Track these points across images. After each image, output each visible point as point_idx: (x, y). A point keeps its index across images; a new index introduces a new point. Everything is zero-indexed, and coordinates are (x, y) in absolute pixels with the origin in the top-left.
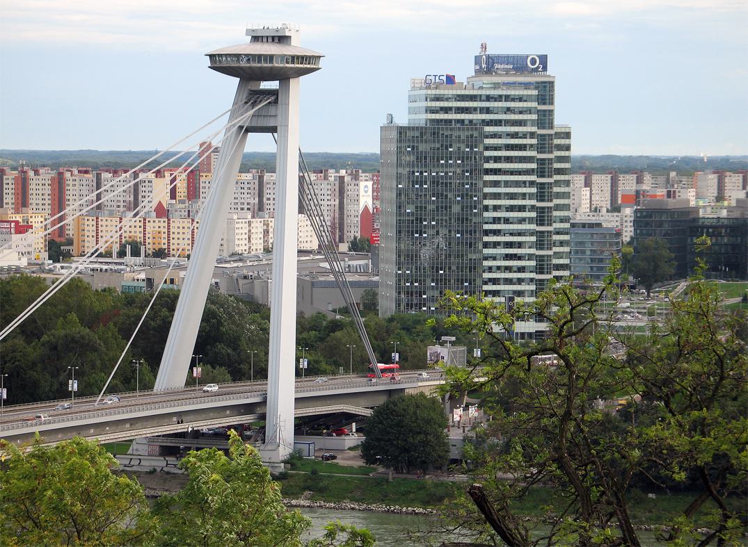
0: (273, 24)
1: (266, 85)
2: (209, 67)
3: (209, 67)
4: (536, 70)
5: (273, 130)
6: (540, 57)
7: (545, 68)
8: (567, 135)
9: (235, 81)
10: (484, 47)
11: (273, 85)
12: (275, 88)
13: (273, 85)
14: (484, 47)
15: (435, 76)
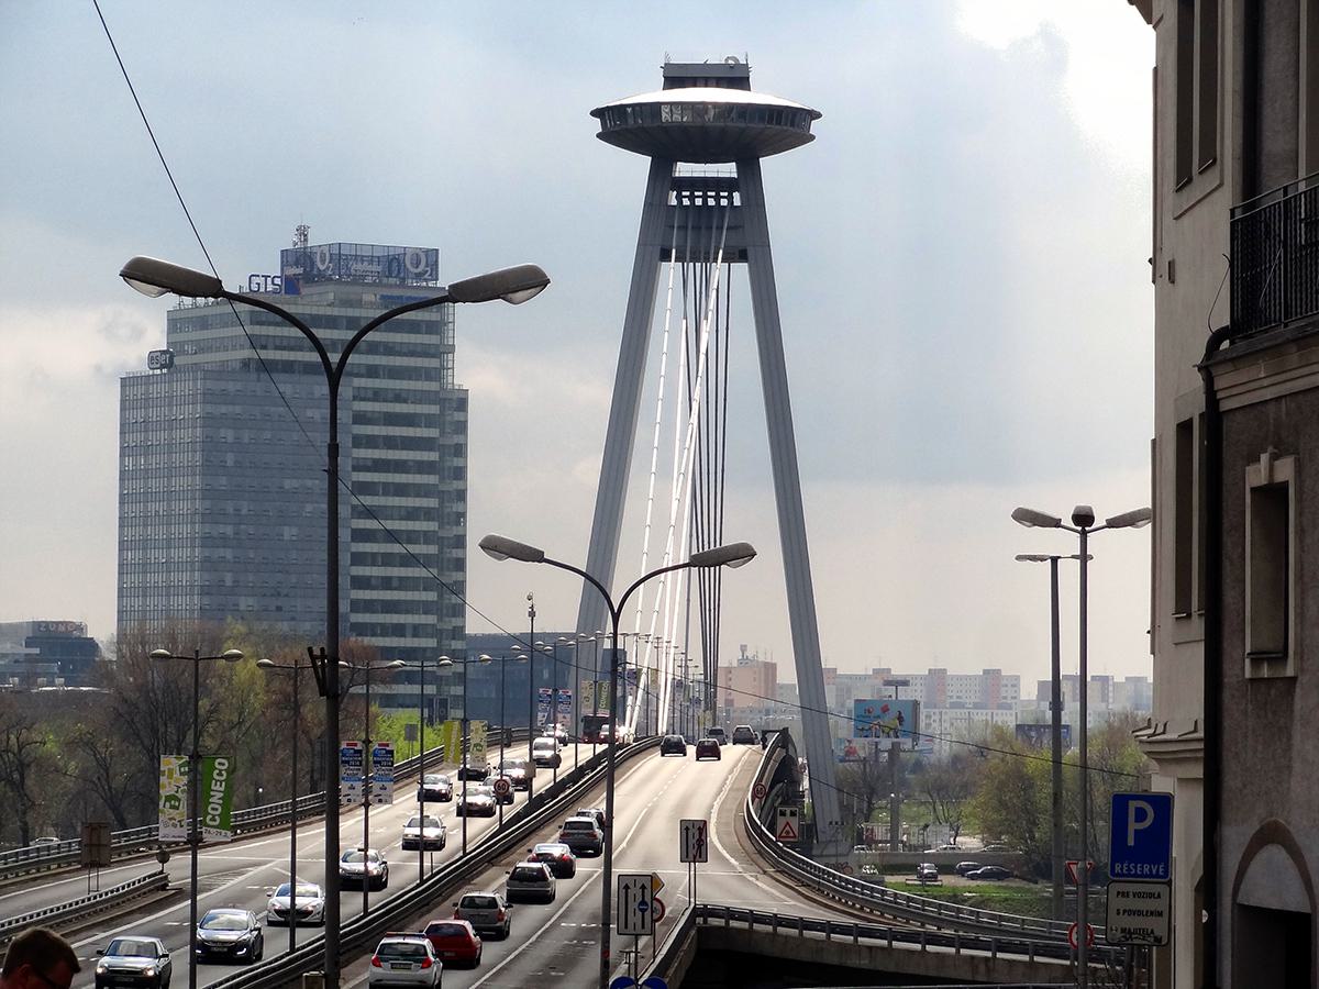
0: (712, 54)
1: (684, 169)
2: (599, 136)
3: (599, 136)
4: (419, 276)
5: (742, 256)
6: (427, 251)
7: (437, 280)
8: (462, 403)
9: (642, 164)
10: (303, 232)
11: (728, 170)
12: (727, 175)
13: (728, 170)
14: (303, 232)
15: (266, 277)
